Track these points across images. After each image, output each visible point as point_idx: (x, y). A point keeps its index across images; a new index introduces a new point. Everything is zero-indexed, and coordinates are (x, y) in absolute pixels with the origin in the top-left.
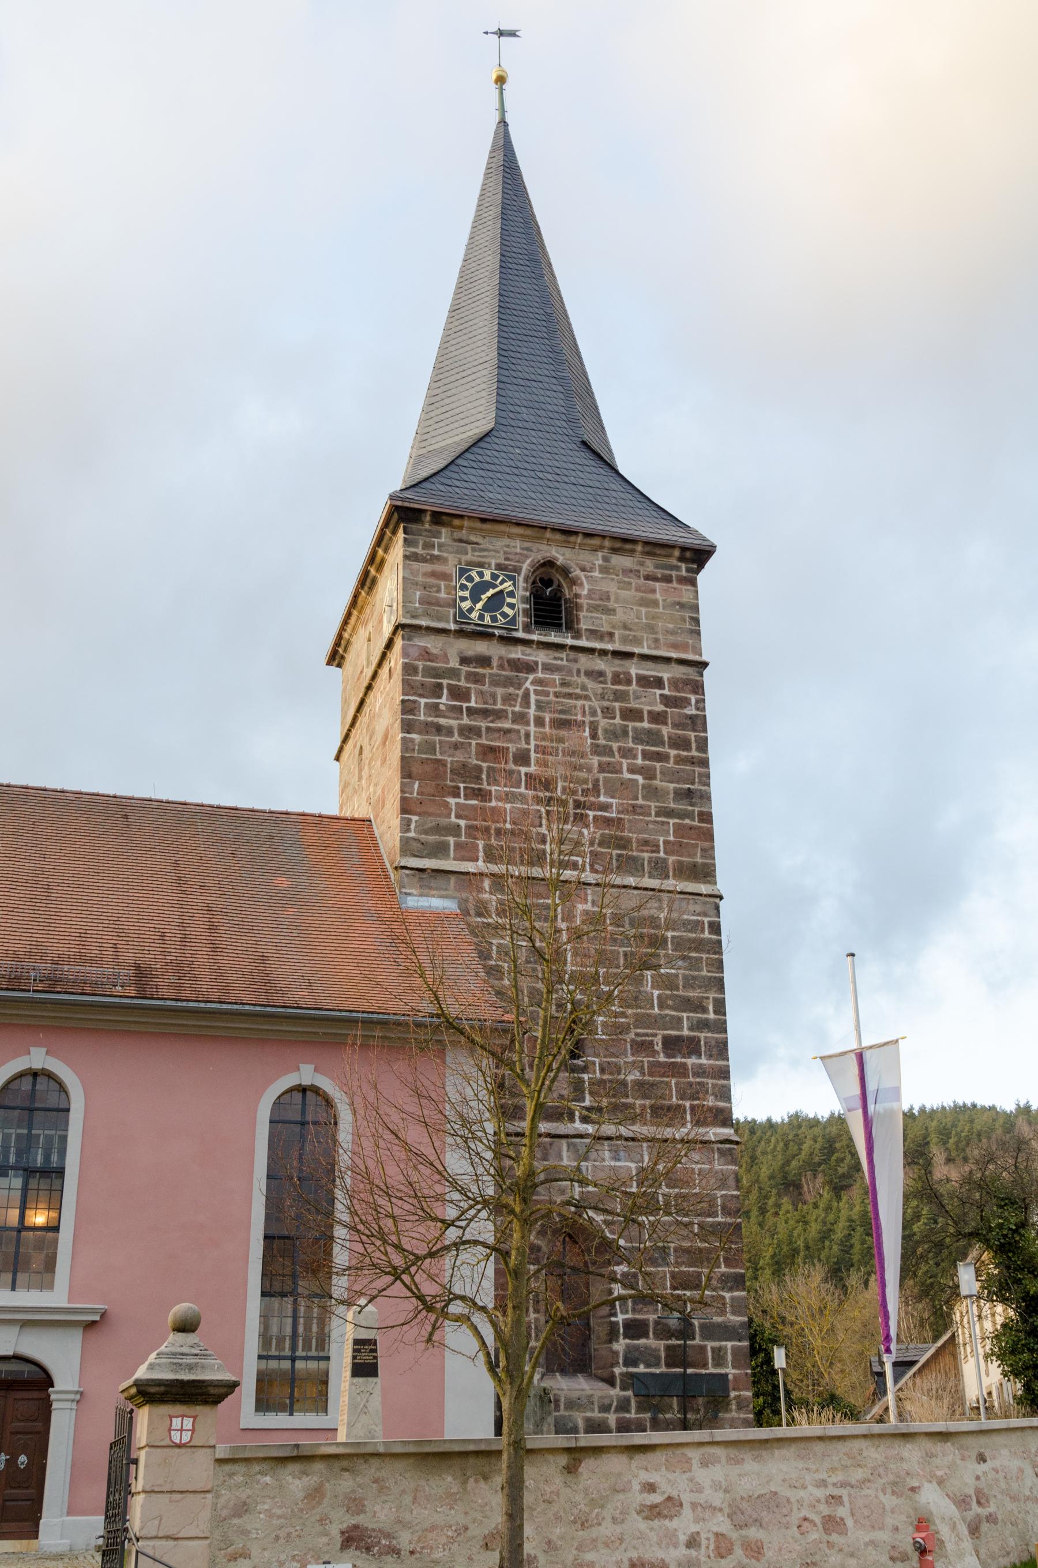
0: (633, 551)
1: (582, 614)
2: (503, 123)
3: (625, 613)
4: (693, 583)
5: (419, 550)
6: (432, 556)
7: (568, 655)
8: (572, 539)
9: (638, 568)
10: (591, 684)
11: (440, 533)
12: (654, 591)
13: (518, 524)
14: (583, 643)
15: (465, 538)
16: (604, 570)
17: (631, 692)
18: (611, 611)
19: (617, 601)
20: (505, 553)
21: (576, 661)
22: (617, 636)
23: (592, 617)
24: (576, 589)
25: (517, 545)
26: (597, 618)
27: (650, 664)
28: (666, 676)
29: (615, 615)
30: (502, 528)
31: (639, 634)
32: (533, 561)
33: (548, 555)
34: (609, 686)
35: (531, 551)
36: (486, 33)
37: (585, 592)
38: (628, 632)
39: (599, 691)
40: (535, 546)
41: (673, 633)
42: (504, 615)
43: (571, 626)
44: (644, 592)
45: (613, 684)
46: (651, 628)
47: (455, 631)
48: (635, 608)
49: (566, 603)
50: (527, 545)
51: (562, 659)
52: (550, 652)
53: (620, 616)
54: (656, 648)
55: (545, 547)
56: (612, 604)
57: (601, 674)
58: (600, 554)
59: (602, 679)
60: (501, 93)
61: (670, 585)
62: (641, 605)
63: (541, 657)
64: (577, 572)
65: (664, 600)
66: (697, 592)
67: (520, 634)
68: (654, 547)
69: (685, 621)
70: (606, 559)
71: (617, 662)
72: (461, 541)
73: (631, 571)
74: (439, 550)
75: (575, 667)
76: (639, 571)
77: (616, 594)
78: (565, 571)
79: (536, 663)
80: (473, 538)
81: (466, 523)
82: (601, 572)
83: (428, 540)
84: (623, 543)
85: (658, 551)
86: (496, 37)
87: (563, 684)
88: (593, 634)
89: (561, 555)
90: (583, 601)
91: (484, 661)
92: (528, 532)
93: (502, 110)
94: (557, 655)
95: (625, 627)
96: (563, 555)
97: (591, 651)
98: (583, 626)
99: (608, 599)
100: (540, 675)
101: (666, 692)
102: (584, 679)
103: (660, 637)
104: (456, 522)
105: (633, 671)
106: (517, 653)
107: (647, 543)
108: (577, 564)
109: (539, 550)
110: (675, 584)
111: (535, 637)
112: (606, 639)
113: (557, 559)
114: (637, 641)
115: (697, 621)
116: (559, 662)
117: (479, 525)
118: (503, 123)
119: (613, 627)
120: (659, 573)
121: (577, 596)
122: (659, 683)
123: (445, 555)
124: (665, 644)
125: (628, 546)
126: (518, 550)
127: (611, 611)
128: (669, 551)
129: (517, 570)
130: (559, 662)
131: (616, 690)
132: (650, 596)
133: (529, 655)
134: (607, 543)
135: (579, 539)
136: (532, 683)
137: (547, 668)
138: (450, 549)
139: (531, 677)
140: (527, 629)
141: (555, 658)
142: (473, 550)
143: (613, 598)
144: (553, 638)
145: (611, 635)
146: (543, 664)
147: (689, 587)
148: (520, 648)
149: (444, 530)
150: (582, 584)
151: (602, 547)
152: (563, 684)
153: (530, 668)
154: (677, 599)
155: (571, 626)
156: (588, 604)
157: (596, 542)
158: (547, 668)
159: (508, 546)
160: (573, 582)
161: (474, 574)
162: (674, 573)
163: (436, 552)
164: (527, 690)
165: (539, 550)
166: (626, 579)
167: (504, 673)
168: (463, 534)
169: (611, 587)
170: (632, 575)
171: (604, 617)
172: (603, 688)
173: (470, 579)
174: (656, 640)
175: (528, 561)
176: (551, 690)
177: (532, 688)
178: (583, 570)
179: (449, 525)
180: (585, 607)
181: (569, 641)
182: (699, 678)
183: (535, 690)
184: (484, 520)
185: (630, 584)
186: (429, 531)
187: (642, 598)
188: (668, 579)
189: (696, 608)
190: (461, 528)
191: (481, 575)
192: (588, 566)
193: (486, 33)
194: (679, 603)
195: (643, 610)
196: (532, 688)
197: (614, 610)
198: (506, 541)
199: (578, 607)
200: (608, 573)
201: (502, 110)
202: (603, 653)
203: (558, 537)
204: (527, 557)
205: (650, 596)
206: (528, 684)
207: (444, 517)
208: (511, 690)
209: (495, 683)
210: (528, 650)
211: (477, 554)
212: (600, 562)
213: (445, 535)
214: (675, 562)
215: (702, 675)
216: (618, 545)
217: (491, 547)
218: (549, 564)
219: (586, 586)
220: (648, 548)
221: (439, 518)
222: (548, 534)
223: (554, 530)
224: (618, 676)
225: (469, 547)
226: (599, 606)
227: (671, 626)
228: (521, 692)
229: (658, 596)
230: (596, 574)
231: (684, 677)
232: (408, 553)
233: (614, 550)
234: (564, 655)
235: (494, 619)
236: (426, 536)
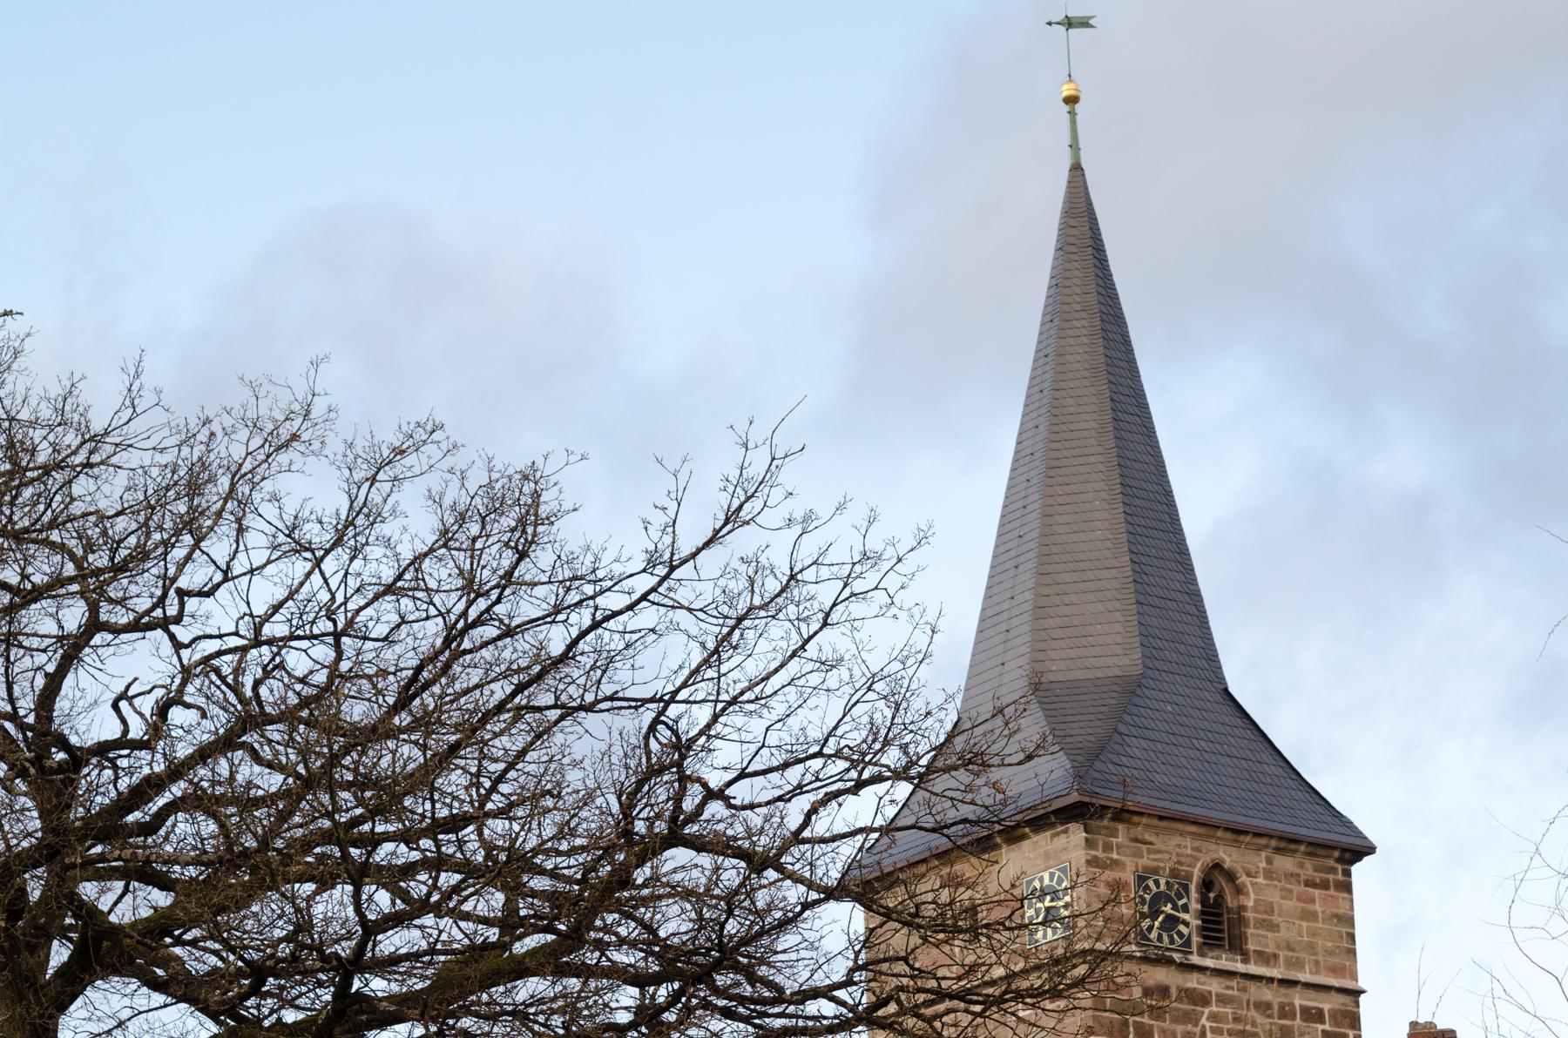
0: (1296, 851)
1: (1250, 931)
2: (1077, 168)
3: (1288, 929)
4: (1347, 887)
5: (1099, 853)
6: (1111, 860)
7: (1238, 983)
8: (1242, 838)
9: (1297, 871)
10: (1260, 1019)
11: (1117, 830)
12: (1312, 901)
13: (1194, 823)
14: (1253, 969)
15: (1140, 837)
16: (1269, 874)
17: (1296, 1028)
18: (1274, 927)
19: (1280, 916)
20: (1178, 855)
21: (1244, 990)
22: (1281, 959)
23: (1258, 935)
24: (1243, 900)
25: (1188, 844)
26: (1263, 936)
27: (1312, 994)
28: (1326, 1007)
29: (1279, 932)
30: (1178, 826)
31: (1302, 955)
32: (1202, 864)
33: (1216, 856)
34: (1276, 1020)
35: (1201, 851)
36: (1050, 24)
37: (1251, 904)
38: (1291, 954)
39: (1268, 1027)
40: (1204, 845)
41: (1331, 953)
42: (1180, 934)
43: (1237, 946)
44: (1304, 902)
45: (1279, 1019)
46: (1312, 948)
47: (1140, 958)
48: (1297, 922)
49: (1228, 913)
50: (1197, 843)
51: (1233, 988)
52: (1221, 980)
53: (1284, 934)
54: (1317, 973)
55: (1212, 847)
56: (1276, 918)
57: (1268, 1006)
58: (1264, 854)
59: (1269, 1012)
60: (1073, 123)
61: (1328, 892)
62: (1302, 919)
63: (1214, 986)
64: (1243, 879)
65: (1323, 912)
66: (1352, 900)
67: (1195, 959)
68: (1317, 848)
69: (1341, 937)
70: (1269, 861)
71: (1283, 990)
72: (1136, 840)
73: (1292, 875)
74: (1118, 854)
75: (1245, 997)
76: (1298, 875)
77: (1279, 905)
78: (1231, 876)
79: (1210, 993)
80: (1148, 837)
81: (1144, 820)
82: (1265, 878)
83: (1107, 839)
84: (1288, 843)
85: (1321, 852)
86: (1063, 29)
87: (1236, 1019)
88: (1266, 958)
89: (1229, 856)
90: (1250, 915)
91: (1164, 991)
92: (1202, 830)
93: (1074, 146)
94: (1229, 983)
95: (1289, 948)
96: (1230, 856)
97: (1259, 978)
98: (1251, 947)
99: (1272, 911)
100: (1214, 1009)
101: (1327, 1027)
102: (1253, 1013)
103: (1320, 958)
104: (1136, 819)
105: (1297, 1002)
106: (1193, 982)
107: (1310, 844)
108: (1243, 868)
109: (1208, 850)
110: (1332, 892)
111: (1209, 962)
112: (1272, 962)
113: (1224, 861)
114: (1298, 964)
115: (1352, 937)
116: (1230, 992)
117: (1156, 822)
118: (1077, 168)
119: (1278, 947)
120: (1318, 877)
121: (1242, 908)
122: (1318, 1016)
123: (1123, 859)
124: (1325, 968)
125: (1293, 846)
126: (1189, 851)
127: (1274, 927)
128: (1329, 852)
129: (1189, 877)
130: (1230, 992)
131: (1283, 1026)
132: (1310, 907)
133: (1204, 984)
134: (1273, 843)
135: (1248, 839)
136: (1208, 1018)
137: (1223, 1000)
138: (1128, 852)
139: (1207, 1011)
140: (1201, 954)
141: (1228, 988)
142: (1149, 852)
143: (1276, 911)
144: (1224, 963)
145: (1275, 956)
146: (1217, 995)
147: (1346, 895)
148: (1195, 975)
149: (1121, 827)
150: (1247, 894)
151: (1266, 846)
152: (1236, 1019)
153: (1204, 999)
154: (1334, 910)
155: (1237, 946)
156: (1255, 918)
157: (1263, 841)
158: (1223, 1000)
159: (1179, 846)
160: (1239, 891)
161: (1151, 884)
162: (1331, 877)
163: (1115, 856)
164: (1204, 1026)
165: (1208, 850)
166: (1288, 886)
167: (1182, 1006)
168: (1138, 831)
169: (1273, 896)
170: (1293, 880)
171: (1269, 934)
172: (1271, 1024)
173: (1147, 888)
174: (1317, 963)
175: (1199, 865)
176: (1226, 1027)
177: (1208, 1025)
178: (1249, 875)
179: (1128, 822)
180: (1252, 923)
181: (1240, 967)
182: (1355, 1010)
183: (1211, 1027)
184: (1161, 818)
185: (1291, 891)
186: (1107, 828)
187: (1303, 910)
188: (1325, 885)
189: (1350, 921)
190: (1138, 824)
191: (1157, 883)
192: (1253, 869)
193: (1050, 24)
194: (1336, 916)
195: (1305, 924)
196: (1208, 1025)
197: (1278, 926)
198: (1178, 839)
199: (1242, 921)
200: (1272, 878)
201: (1074, 146)
202: (1271, 980)
203: (1229, 835)
204: (1198, 859)
205: (1310, 907)
206: (1204, 1021)
207: (1126, 816)
208: (1189, 1027)
209: (1175, 1020)
210: (1203, 978)
211: (1152, 856)
212: (1263, 865)
213: (1122, 835)
214: (1331, 863)
215: (1357, 1005)
216: (1283, 845)
217: (1164, 848)
218: (1217, 866)
219: (1252, 896)
220: (1310, 849)
221: (1122, 815)
222: (1220, 833)
223: (1227, 829)
224: (1284, 1009)
225: (1144, 847)
226: (1264, 920)
227: (1330, 944)
228: (1198, 1030)
229: (1318, 907)
230: (1260, 880)
231: (1343, 1008)
232: (1089, 858)
233: (1278, 850)
234: (1234, 984)
235: (1172, 941)
236: (1107, 836)
